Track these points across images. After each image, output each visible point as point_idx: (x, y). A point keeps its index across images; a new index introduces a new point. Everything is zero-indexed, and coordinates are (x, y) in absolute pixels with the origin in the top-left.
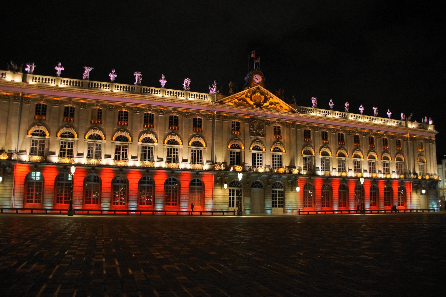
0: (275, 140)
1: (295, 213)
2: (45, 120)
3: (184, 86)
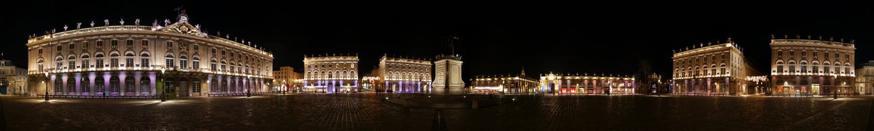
1: (207, 96)
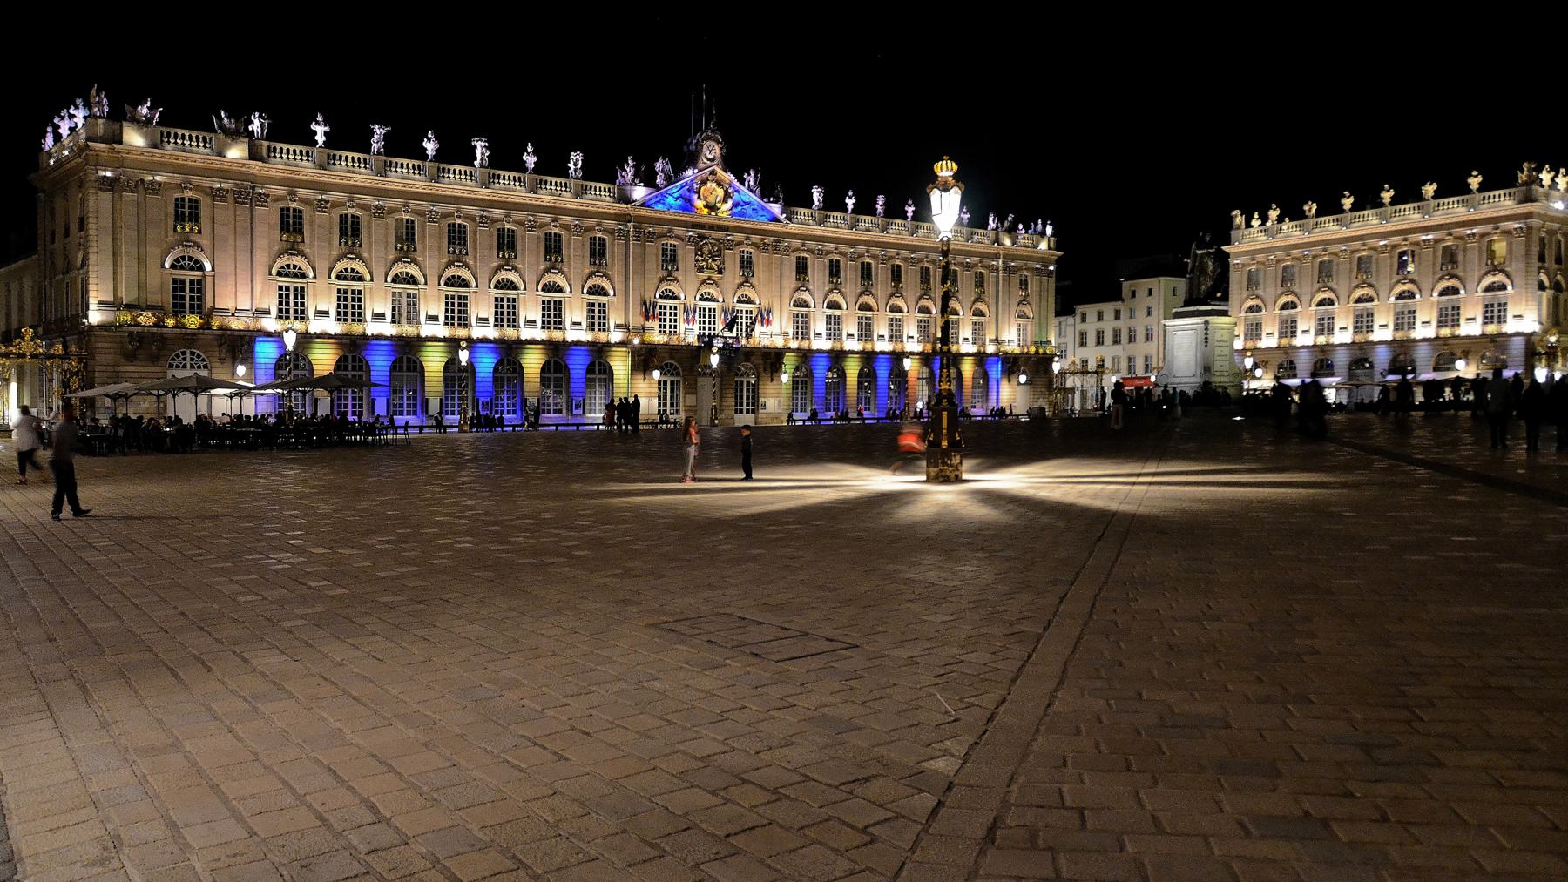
0: (742, 280)
2: (303, 242)
3: (570, 168)
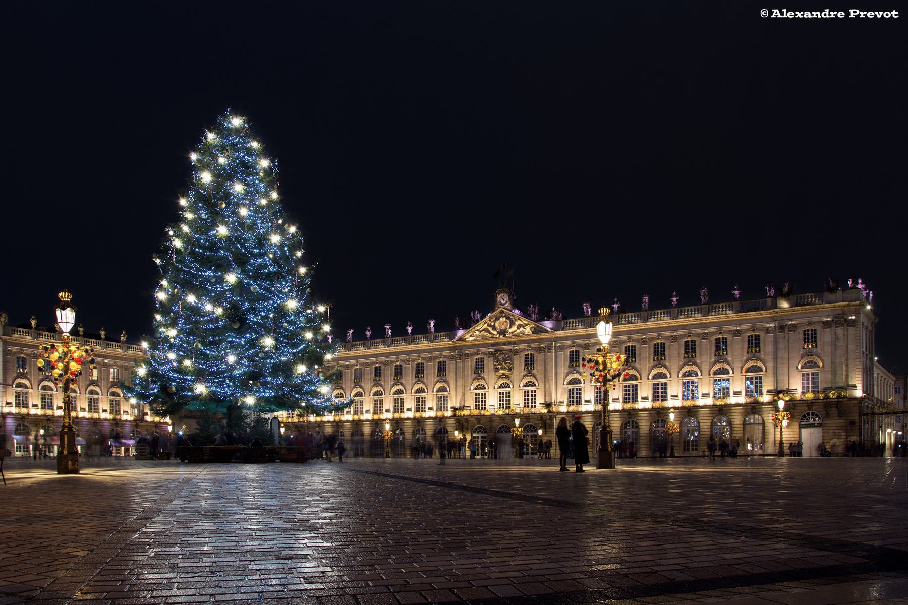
0: (526, 372)
